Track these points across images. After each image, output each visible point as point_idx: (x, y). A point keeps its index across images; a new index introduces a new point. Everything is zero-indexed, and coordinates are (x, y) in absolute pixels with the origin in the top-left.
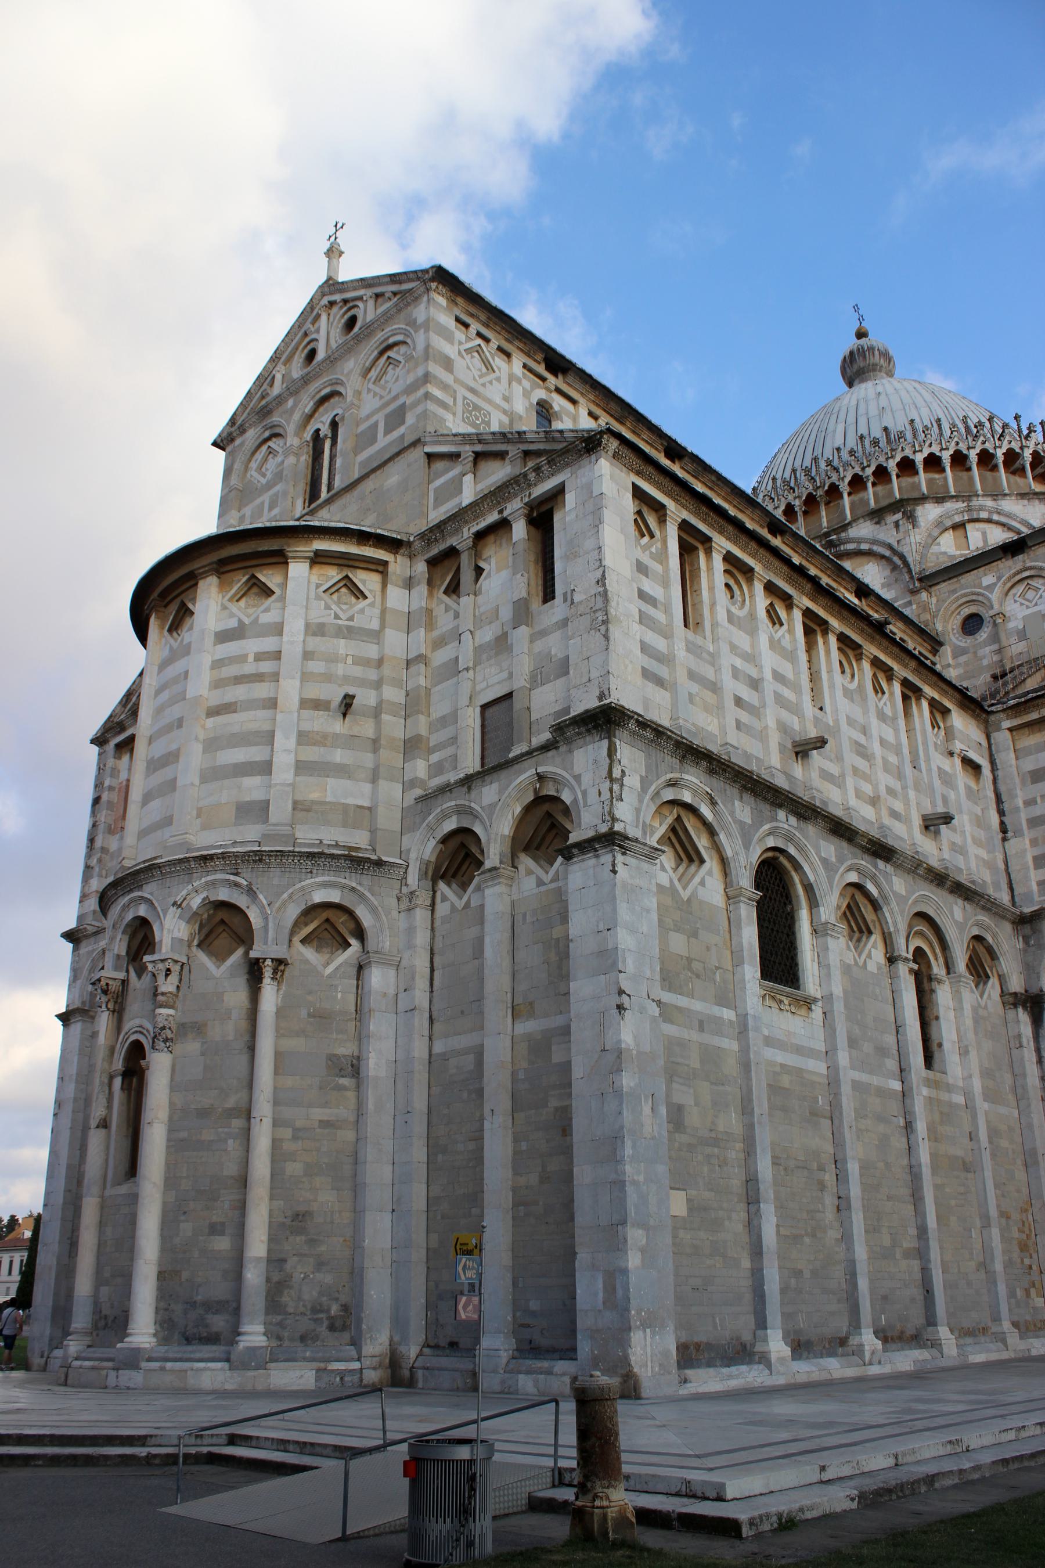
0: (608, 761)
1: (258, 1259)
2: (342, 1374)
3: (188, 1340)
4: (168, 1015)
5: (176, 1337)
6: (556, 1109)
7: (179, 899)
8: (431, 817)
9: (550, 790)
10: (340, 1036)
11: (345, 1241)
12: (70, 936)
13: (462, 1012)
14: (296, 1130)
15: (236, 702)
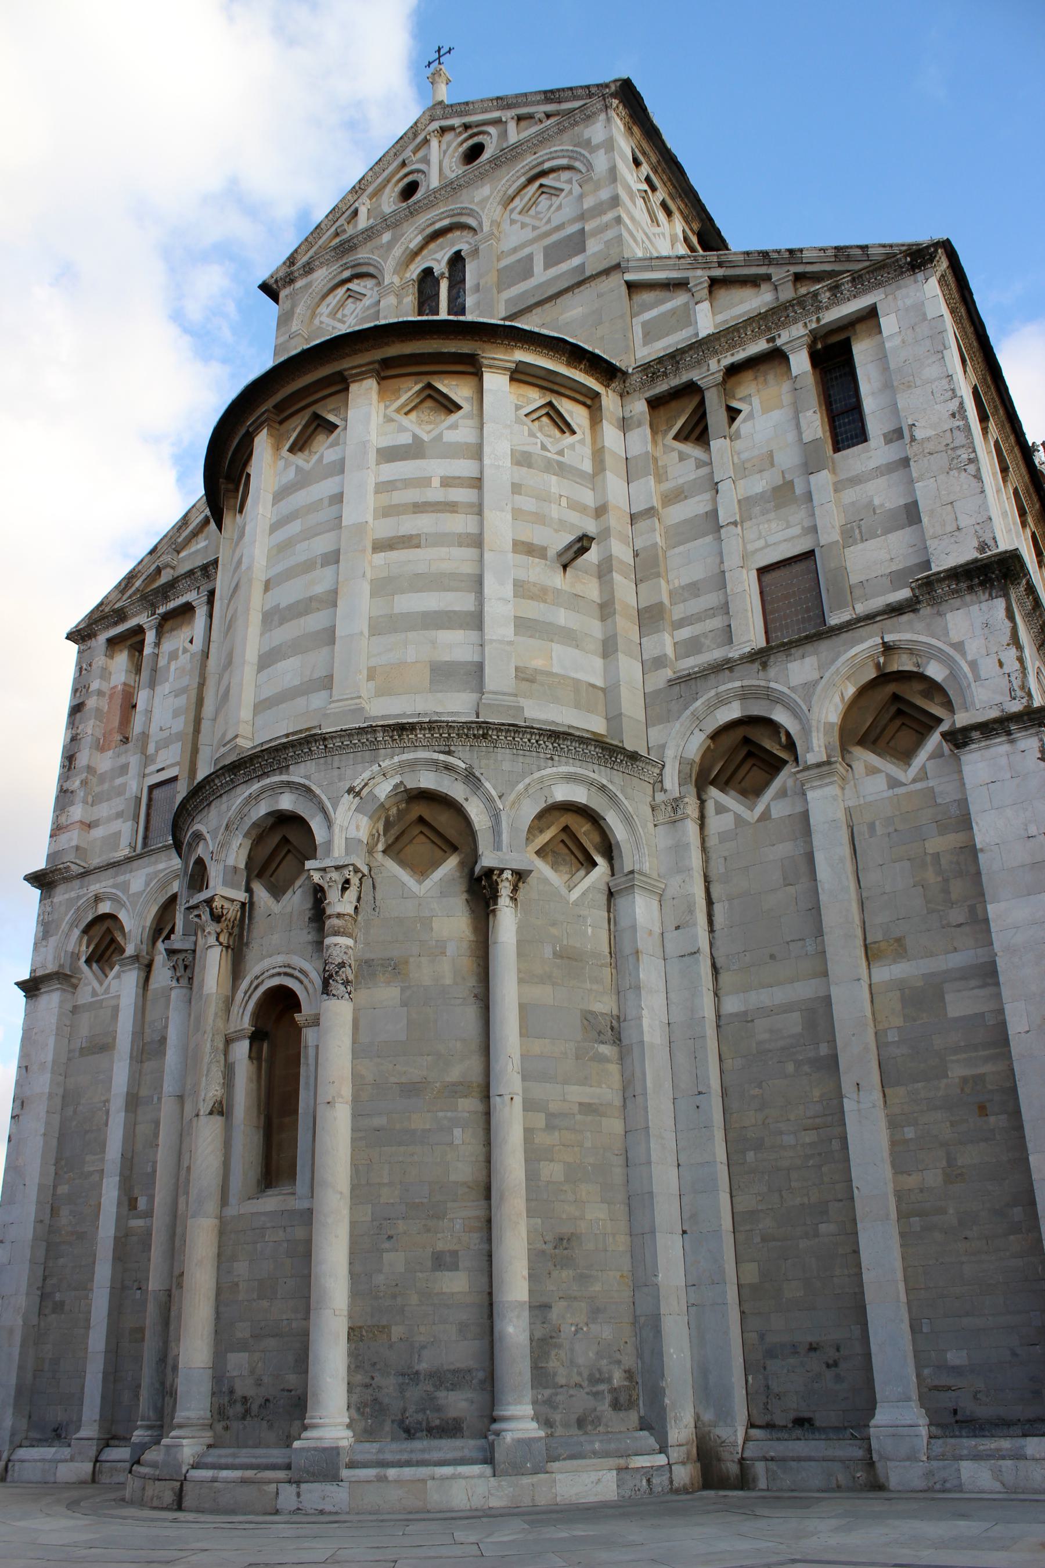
0: (1008, 624)
1: (521, 1304)
2: (649, 1474)
3: (409, 1433)
4: (348, 947)
5: (388, 1427)
6: (964, 1080)
7: (357, 783)
8: (698, 703)
9: (904, 663)
10: (595, 987)
11: (622, 1276)
12: (40, 880)
13: (772, 957)
14: (550, 1116)
15: (419, 535)
